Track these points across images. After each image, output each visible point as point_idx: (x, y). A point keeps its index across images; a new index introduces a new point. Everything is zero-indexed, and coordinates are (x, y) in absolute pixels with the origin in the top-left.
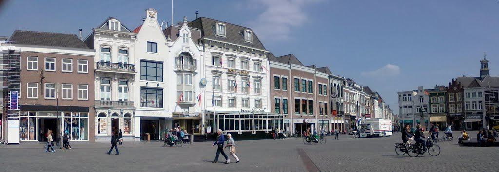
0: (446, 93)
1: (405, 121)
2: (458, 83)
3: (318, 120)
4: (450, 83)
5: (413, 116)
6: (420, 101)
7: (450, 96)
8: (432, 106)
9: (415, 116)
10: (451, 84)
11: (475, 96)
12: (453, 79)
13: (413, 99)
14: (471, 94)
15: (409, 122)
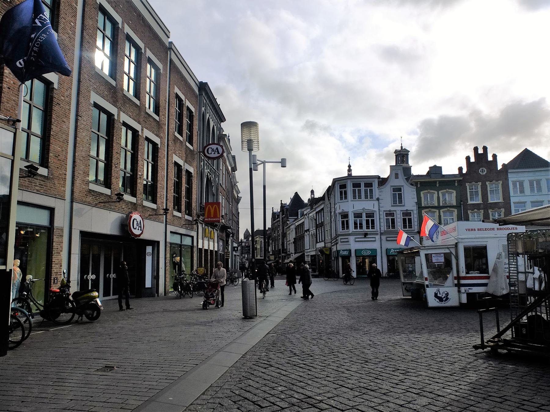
0: (459, 181)
2: (490, 158)
4: (468, 158)
5: (378, 237)
6: (395, 202)
7: (468, 190)
8: (423, 211)
9: (384, 237)
10: (472, 160)
11: (540, 189)
12: (476, 149)
14: (527, 185)
15: (369, 253)
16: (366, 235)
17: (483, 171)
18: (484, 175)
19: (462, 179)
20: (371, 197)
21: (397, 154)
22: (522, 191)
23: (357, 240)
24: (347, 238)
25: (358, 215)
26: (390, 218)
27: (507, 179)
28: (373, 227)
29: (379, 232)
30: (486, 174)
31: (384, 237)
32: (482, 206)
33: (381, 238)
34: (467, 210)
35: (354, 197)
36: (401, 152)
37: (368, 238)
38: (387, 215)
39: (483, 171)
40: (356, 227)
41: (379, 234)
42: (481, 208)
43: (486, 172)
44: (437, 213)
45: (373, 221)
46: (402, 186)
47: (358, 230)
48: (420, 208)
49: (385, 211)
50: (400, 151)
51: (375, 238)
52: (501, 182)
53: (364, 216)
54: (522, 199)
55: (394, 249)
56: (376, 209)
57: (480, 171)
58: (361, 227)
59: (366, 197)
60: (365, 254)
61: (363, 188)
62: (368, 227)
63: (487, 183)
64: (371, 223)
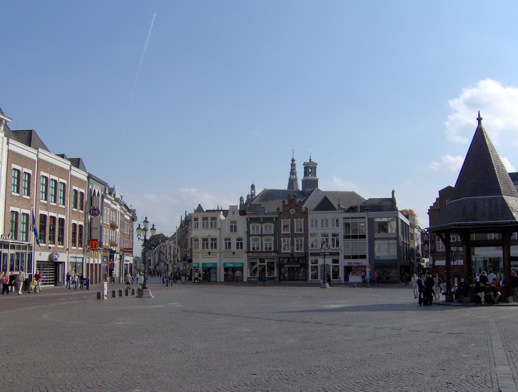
0: (276, 218)
1: (203, 264)
3: (70, 255)
5: (218, 255)
6: (231, 231)
8: (251, 238)
11: (327, 225)
13: (219, 225)
15: (211, 266)
16: (209, 253)
17: (292, 211)
19: (278, 216)
20: (215, 227)
21: (306, 166)
22: (316, 226)
23: (204, 256)
24: (197, 255)
25: (205, 240)
26: (228, 242)
27: (307, 217)
28: (215, 248)
29: (219, 251)
31: (222, 255)
32: (290, 235)
33: (220, 255)
34: (281, 237)
35: (203, 227)
36: (309, 165)
37: (212, 255)
38: (226, 239)
39: (292, 211)
40: (203, 248)
41: (219, 253)
44: (260, 240)
45: (215, 244)
46: (237, 220)
47: (205, 249)
48: (249, 235)
49: (224, 237)
50: (307, 164)
51: (216, 255)
52: (303, 219)
53: (209, 240)
54: (316, 232)
55: (228, 263)
56: (218, 235)
57: (290, 211)
58: (207, 248)
59: (212, 227)
60: (208, 266)
61: (209, 221)
62: (212, 248)
64: (214, 246)
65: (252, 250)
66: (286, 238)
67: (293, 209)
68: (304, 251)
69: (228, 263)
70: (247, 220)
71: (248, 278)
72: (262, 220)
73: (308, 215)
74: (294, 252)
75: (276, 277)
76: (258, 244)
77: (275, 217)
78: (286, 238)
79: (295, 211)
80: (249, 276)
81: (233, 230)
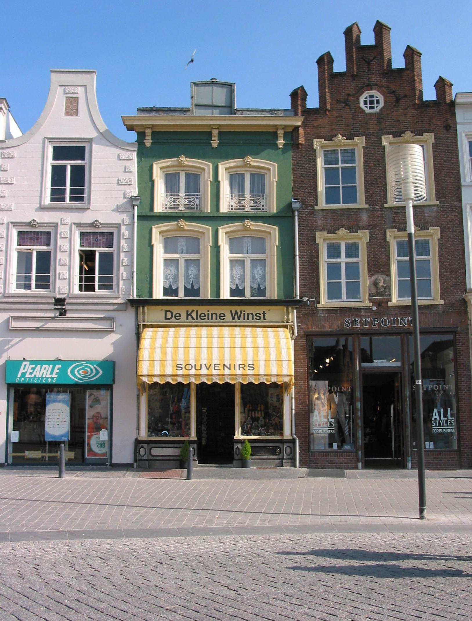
17: (372, 102)
18: (375, 114)
26: (35, 249)
30: (381, 110)
32: (365, 217)
38: (23, 237)
39: (372, 102)
42: (361, 224)
43: (382, 104)
57: (362, 100)
63: (386, 140)
65: (164, 296)
66: (342, 231)
67: (375, 93)
68: (442, 298)
69: (32, 362)
70: (140, 141)
71: (138, 443)
72: (215, 143)
73: (453, 114)
74: (390, 304)
75: (293, 441)
76: (197, 262)
77: (285, 127)
78: (342, 231)
79: (385, 102)
80: (144, 434)
81: (63, 192)
